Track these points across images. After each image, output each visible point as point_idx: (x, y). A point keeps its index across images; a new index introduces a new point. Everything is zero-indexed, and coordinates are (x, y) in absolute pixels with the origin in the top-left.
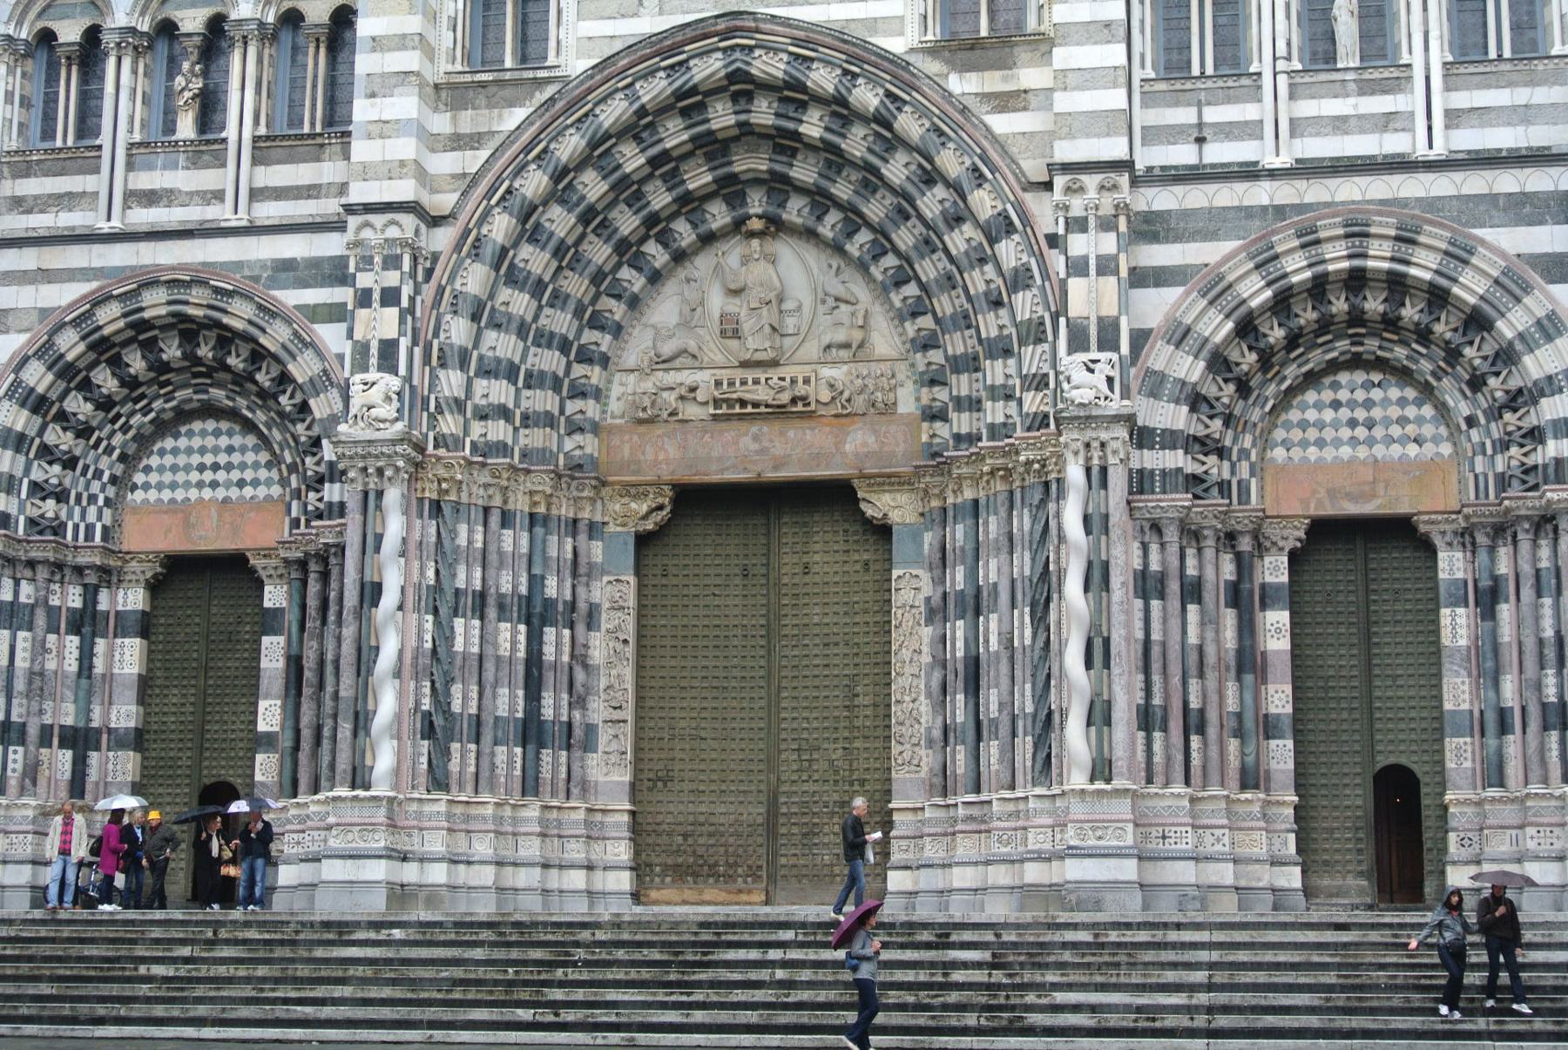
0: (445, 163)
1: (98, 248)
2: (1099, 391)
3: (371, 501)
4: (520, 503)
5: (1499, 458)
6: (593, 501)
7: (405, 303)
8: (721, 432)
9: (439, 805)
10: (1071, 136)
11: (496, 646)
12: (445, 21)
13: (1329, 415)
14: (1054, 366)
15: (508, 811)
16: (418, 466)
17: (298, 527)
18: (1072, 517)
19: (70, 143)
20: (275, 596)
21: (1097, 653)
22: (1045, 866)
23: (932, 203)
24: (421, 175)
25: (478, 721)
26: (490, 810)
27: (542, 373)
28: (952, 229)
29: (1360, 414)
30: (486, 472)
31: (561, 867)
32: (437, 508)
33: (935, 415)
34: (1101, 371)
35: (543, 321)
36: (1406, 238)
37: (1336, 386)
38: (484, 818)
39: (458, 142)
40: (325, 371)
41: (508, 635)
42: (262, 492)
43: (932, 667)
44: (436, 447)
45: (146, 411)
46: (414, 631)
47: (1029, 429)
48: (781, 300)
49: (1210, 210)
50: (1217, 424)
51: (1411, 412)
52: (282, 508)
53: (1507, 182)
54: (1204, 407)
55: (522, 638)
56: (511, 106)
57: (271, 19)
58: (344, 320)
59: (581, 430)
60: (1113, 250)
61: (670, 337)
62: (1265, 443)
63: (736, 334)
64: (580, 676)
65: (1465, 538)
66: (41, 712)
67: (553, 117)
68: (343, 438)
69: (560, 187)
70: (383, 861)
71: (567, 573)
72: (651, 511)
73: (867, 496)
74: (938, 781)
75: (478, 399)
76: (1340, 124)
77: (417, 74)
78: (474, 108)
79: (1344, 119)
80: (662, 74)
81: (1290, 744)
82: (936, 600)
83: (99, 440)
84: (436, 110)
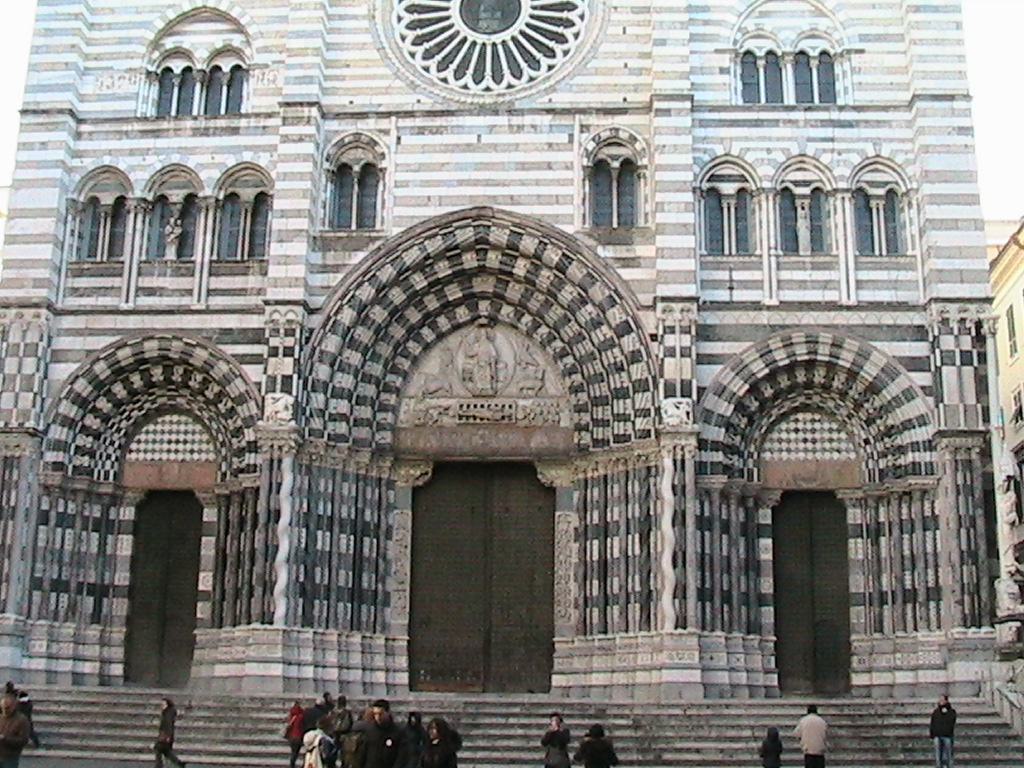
0: (318, 280)
1: (120, 318)
3: (274, 465)
5: (880, 461)
7: (296, 356)
9: (308, 633)
10: (666, 283)
13: (793, 436)
14: (653, 404)
15: (344, 638)
18: (665, 485)
19: (105, 259)
20: (210, 515)
21: (679, 559)
22: (647, 674)
25: (328, 588)
26: (334, 638)
29: (809, 436)
31: (372, 670)
33: (579, 428)
35: (366, 368)
36: (837, 345)
37: (797, 421)
39: (325, 269)
45: (140, 409)
48: (496, 363)
50: (738, 438)
51: (835, 436)
52: (214, 467)
53: (888, 318)
54: (732, 430)
55: (352, 543)
57: (221, 197)
58: (261, 363)
60: (688, 344)
62: (760, 450)
63: (471, 379)
65: (862, 503)
66: (78, 575)
70: (281, 666)
74: (581, 626)
76: (802, 285)
78: (336, 251)
79: (805, 282)
81: (772, 609)
82: (581, 530)
83: (114, 424)
84: (313, 250)
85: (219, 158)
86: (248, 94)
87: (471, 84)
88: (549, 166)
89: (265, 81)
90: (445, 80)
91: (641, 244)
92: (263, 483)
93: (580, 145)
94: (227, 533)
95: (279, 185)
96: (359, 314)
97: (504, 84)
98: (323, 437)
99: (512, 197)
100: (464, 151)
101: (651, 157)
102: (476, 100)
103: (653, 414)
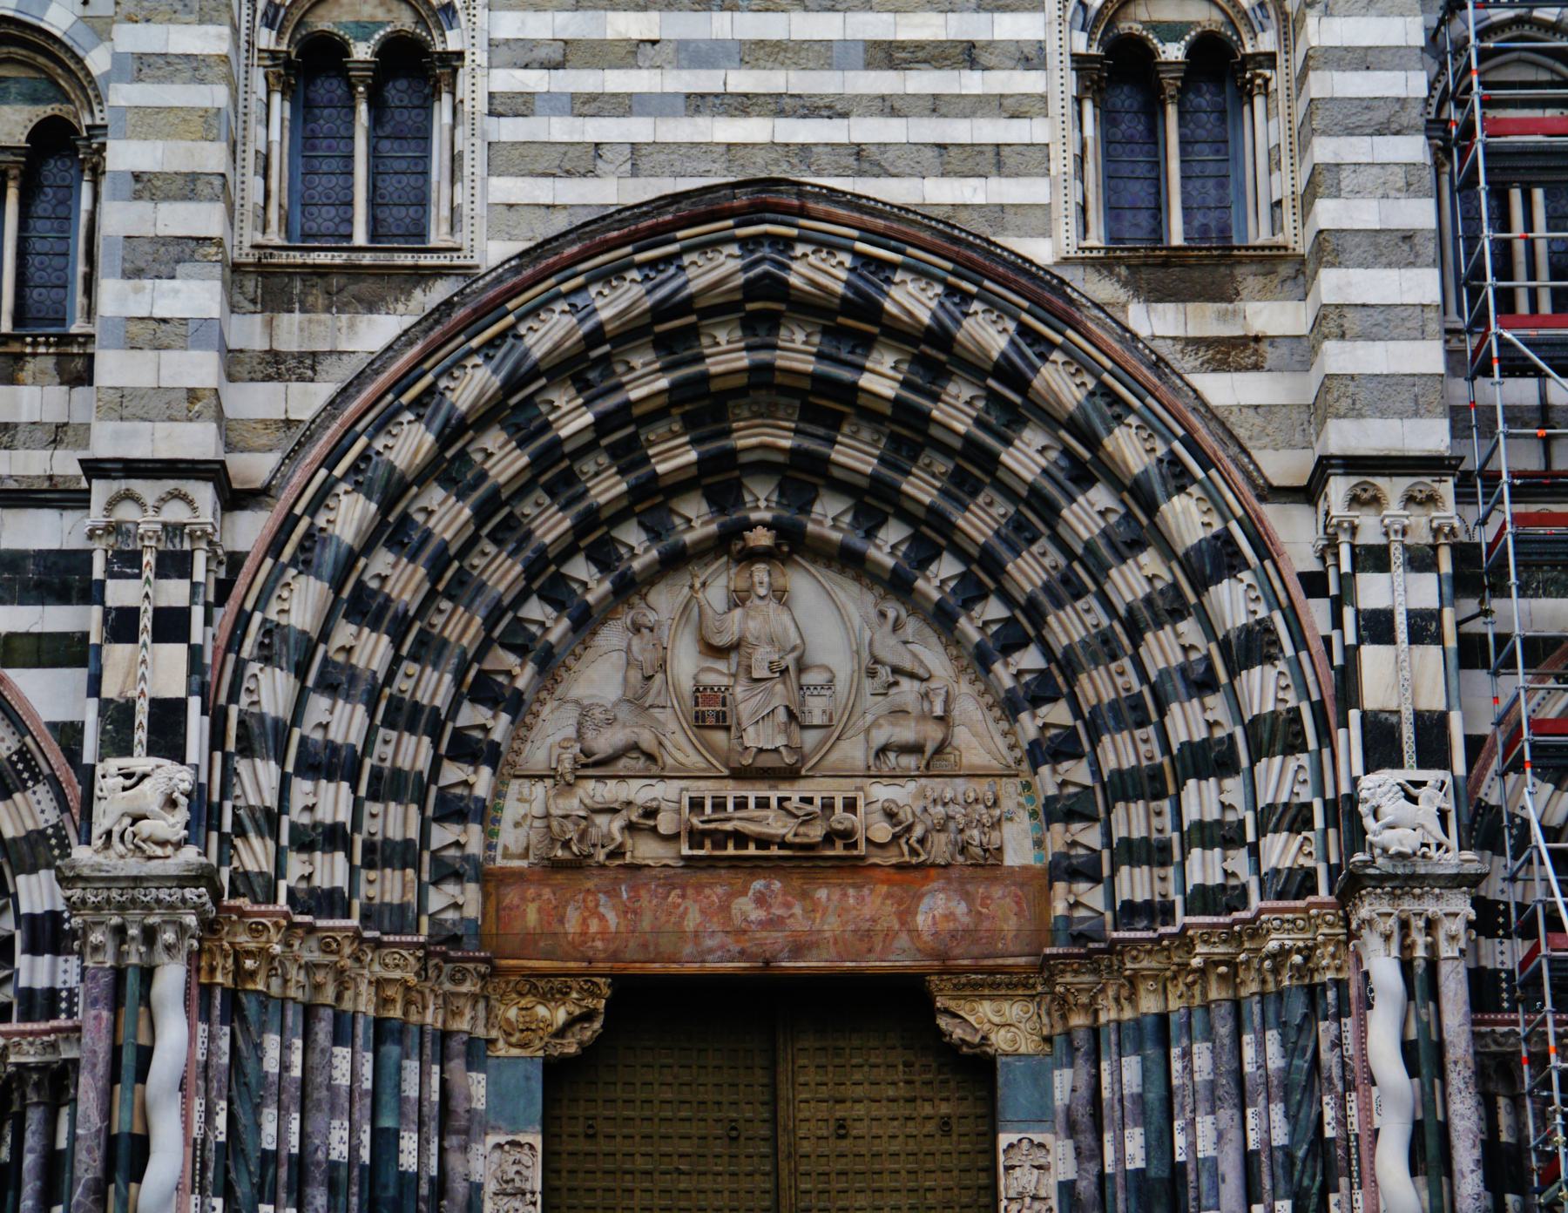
3: (127, 990)
4: (363, 1002)
6: (474, 998)
8: (699, 888)
10: (1354, 412)
12: (251, 156)
14: (1320, 791)
23: (1089, 513)
24: (220, 416)
27: (397, 772)
28: (1123, 560)
30: (313, 943)
32: (234, 1009)
34: (1430, 800)
35: (402, 684)
40: (23, 753)
47: (1280, 896)
48: (802, 667)
56: (371, 311)
59: (458, 877)
60: (1434, 603)
61: (610, 722)
63: (722, 723)
67: (443, 336)
68: (86, 872)
69: (449, 454)
71: (432, 1127)
73: (952, 1005)
75: (297, 815)
77: (219, 243)
78: (303, 310)
80: (635, 274)
82: (1086, 1187)
84: (233, 308)
88: (969, 55)
91: (1264, 294)
92: (93, 1047)
95: (122, 95)
96: (385, 508)
98: (274, 899)
99: (858, 151)
101: (1290, 27)
103: (1319, 822)
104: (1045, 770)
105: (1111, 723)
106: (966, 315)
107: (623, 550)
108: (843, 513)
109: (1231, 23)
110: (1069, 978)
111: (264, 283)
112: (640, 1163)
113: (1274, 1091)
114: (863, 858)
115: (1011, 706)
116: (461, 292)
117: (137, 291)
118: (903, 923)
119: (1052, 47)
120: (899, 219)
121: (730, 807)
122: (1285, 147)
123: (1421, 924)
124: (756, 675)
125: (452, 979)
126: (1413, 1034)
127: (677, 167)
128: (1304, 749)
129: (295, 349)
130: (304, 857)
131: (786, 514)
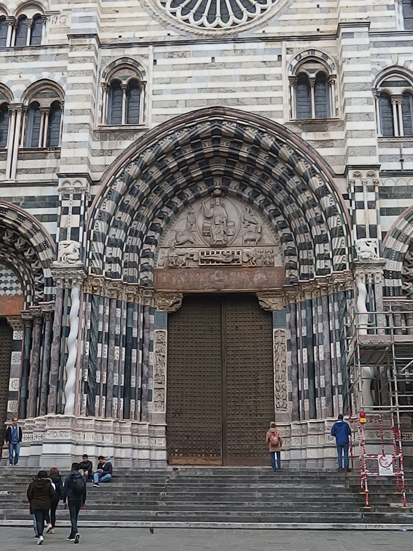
2: (372, 253)
3: (66, 293)
4: (124, 298)
6: (151, 298)
7: (82, 213)
8: (203, 272)
9: (92, 422)
10: (355, 155)
11: (113, 355)
12: (98, 106)
16: (85, 280)
17: (30, 305)
20: (17, 335)
23: (293, 183)
24: (89, 164)
25: (105, 386)
26: (111, 424)
27: (132, 246)
28: (301, 193)
30: (111, 284)
31: (139, 449)
34: (372, 245)
35: (133, 226)
38: (109, 428)
39: (103, 153)
40: (45, 242)
41: (118, 352)
42: (14, 292)
43: (291, 367)
44: (92, 272)
46: (82, 348)
47: (338, 270)
49: (408, 186)
52: (22, 299)
54: (406, 263)
55: (124, 353)
56: (125, 140)
57: (27, 104)
59: (147, 270)
61: (183, 235)
64: (146, 369)
69: (143, 172)
70: (70, 445)
72: (174, 303)
73: (262, 299)
74: (296, 414)
75: (107, 255)
78: (109, 140)
82: (293, 340)
85: (24, 77)
86: (46, 33)
87: (206, 23)
88: (264, 77)
89: (58, 23)
90: (187, 21)
91: (334, 130)
93: (287, 62)
94: (30, 348)
95: (68, 93)
96: (128, 185)
97: (230, 22)
99: (238, 100)
100: (203, 68)
101: (339, 68)
102: (210, 33)
103: (347, 252)
104: (284, 244)
105: (299, 232)
106: (263, 137)
107: (186, 195)
108: (237, 186)
109: (327, 69)
110: (289, 292)
111: (102, 134)
112: (190, 336)
113: (336, 317)
114: (241, 265)
115: (276, 230)
116: (145, 135)
117: (70, 135)
118: (251, 281)
119: (283, 75)
120: (247, 115)
121: (210, 254)
122: (339, 96)
123: (371, 275)
124: (216, 223)
125: (145, 293)
126: (368, 301)
127: (196, 105)
128: (343, 236)
129: (107, 149)
130: (109, 265)
131: (223, 186)
